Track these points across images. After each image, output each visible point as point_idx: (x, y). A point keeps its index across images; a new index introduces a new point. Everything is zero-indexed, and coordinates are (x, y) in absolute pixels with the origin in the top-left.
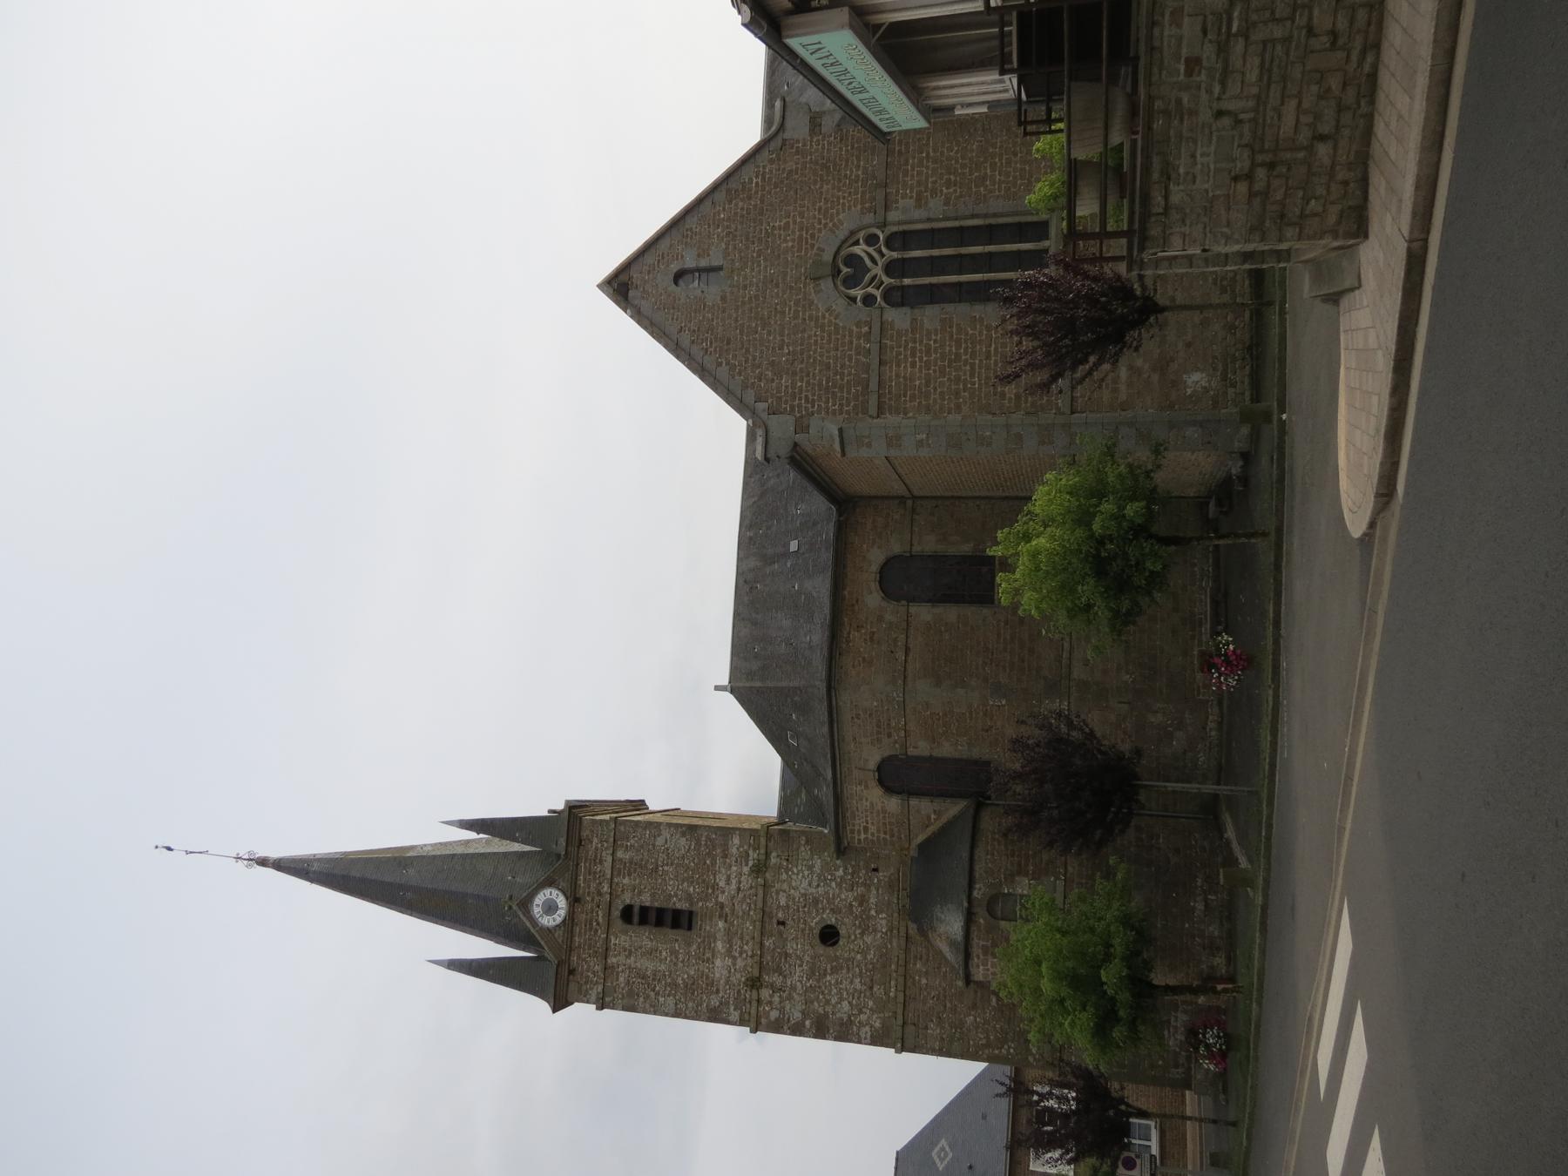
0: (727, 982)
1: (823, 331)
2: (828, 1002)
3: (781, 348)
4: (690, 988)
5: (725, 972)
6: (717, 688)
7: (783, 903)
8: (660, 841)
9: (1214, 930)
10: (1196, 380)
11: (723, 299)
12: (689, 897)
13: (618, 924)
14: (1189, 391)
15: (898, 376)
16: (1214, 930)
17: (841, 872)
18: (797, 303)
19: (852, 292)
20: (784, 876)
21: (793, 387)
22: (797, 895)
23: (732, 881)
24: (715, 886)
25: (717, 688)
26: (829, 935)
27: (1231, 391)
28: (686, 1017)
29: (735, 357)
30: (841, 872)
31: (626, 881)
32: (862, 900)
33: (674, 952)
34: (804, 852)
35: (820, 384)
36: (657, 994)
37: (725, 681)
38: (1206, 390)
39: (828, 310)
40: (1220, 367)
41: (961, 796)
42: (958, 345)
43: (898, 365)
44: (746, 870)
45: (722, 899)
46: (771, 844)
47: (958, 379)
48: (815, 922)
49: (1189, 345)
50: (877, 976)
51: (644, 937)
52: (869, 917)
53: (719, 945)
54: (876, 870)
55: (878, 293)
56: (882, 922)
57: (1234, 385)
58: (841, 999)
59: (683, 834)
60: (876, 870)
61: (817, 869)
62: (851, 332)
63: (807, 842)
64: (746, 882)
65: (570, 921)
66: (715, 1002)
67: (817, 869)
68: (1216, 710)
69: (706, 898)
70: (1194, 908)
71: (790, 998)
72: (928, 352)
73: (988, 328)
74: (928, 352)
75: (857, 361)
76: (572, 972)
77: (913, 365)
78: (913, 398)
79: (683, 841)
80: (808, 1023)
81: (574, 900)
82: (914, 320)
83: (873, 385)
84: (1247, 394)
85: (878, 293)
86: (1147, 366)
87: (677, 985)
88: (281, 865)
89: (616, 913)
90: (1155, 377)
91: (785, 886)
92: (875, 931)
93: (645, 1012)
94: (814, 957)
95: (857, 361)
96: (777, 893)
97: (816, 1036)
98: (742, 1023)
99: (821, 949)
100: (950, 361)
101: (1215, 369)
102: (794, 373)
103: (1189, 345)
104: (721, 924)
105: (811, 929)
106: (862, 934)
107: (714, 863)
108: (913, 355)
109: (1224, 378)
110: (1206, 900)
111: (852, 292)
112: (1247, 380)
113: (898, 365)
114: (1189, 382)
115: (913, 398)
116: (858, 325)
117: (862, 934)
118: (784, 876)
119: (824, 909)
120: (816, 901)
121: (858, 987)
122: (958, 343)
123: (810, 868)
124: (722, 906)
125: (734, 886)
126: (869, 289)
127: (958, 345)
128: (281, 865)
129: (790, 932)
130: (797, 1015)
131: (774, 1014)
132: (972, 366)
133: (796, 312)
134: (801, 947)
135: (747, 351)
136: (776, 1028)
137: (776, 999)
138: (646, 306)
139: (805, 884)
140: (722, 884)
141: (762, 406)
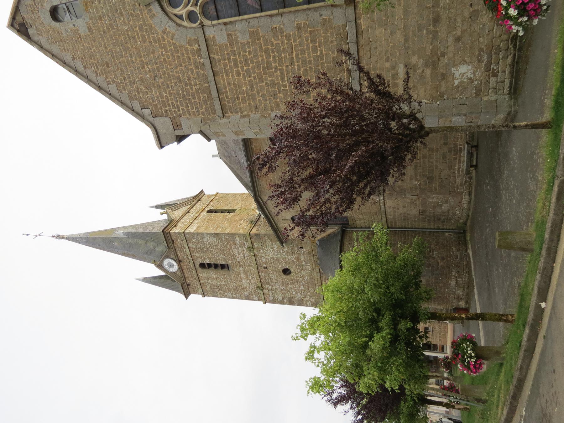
0: (250, 287)
1: (166, 51)
2: (292, 294)
3: (143, 68)
4: (236, 289)
5: (248, 285)
6: (213, 156)
7: (264, 261)
8: (205, 240)
9: (460, 292)
10: (463, 72)
11: (90, 29)
12: (225, 260)
13: (200, 270)
14: (456, 82)
15: (229, 83)
16: (460, 292)
17: (286, 249)
18: (141, 27)
19: (177, 11)
20: (262, 251)
21: (162, 97)
22: (269, 258)
23: (240, 253)
24: (234, 256)
25: (213, 156)
26: (286, 272)
27: (493, 80)
28: (237, 299)
29: (116, 75)
30: (286, 249)
31: (197, 255)
32: (298, 259)
33: (225, 278)
34: (268, 242)
35: (178, 94)
36: (224, 292)
37: (216, 152)
38: (471, 80)
39: (164, 32)
40: (485, 59)
41: (336, 224)
42: (268, 55)
43: (227, 75)
44: (245, 249)
45: (238, 260)
46: (253, 240)
47: (273, 84)
48: (280, 267)
49: (458, 39)
50: (310, 285)
51: (211, 273)
52: (302, 265)
53: (242, 276)
54: (301, 248)
55: (197, 10)
56: (308, 267)
57: (495, 75)
58: (297, 293)
59: (214, 237)
60: (301, 248)
61: (275, 248)
62: (186, 49)
63: (268, 238)
64: (247, 254)
65: (181, 268)
66: (247, 294)
67: (275, 248)
68: (467, 197)
69: (232, 260)
70: (450, 284)
71: (276, 293)
72: (247, 64)
73: (288, 37)
74: (247, 64)
75: (198, 74)
76: (188, 285)
77: (238, 74)
78: (244, 100)
79: (215, 240)
80: (285, 300)
81: (179, 262)
82: (229, 35)
83: (214, 94)
84: (507, 82)
85: (197, 10)
86: (421, 62)
87: (230, 289)
88: (69, 238)
89: (198, 266)
90: (428, 72)
91: (263, 255)
92: (306, 270)
93: (220, 297)
94: (282, 279)
95: (198, 74)
96: (261, 257)
97: (289, 304)
98: (259, 300)
99: (284, 277)
100: (264, 69)
101: (480, 61)
102: (159, 87)
103: (458, 39)
104: (241, 269)
105: (278, 270)
106: (301, 271)
107: (231, 247)
108: (236, 65)
109: (488, 69)
110: (456, 280)
111: (177, 11)
112: (508, 69)
113: (227, 75)
114: (457, 75)
115: (244, 100)
116: (190, 43)
117: (301, 271)
118: (262, 251)
119: (282, 263)
120: (278, 260)
121: (303, 289)
122: (267, 51)
123: (273, 248)
124: (239, 262)
125: (242, 255)
126: (189, 8)
127: (268, 55)
128: (69, 238)
129: (270, 270)
130: (280, 298)
131: (271, 298)
132: (281, 71)
133: (143, 36)
134: (276, 277)
135: (122, 71)
136: (274, 302)
137: (270, 293)
138: (43, 41)
139: (272, 254)
140: (237, 255)
141: (146, 112)
